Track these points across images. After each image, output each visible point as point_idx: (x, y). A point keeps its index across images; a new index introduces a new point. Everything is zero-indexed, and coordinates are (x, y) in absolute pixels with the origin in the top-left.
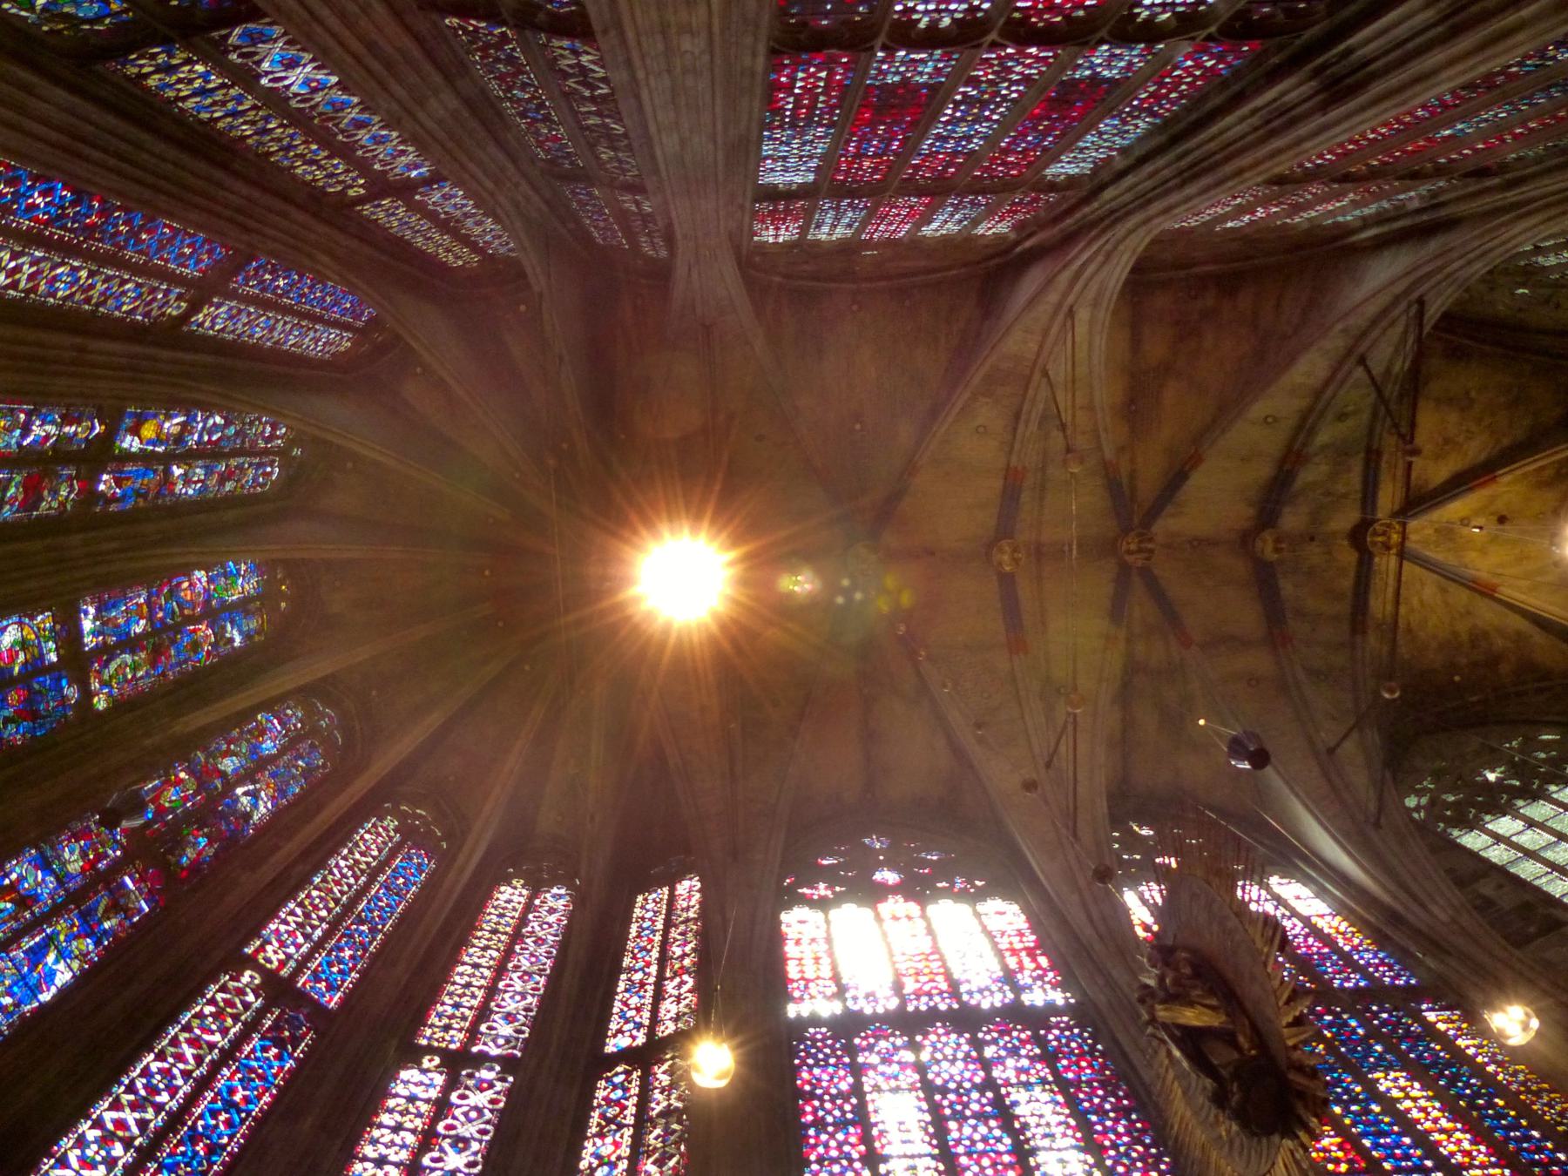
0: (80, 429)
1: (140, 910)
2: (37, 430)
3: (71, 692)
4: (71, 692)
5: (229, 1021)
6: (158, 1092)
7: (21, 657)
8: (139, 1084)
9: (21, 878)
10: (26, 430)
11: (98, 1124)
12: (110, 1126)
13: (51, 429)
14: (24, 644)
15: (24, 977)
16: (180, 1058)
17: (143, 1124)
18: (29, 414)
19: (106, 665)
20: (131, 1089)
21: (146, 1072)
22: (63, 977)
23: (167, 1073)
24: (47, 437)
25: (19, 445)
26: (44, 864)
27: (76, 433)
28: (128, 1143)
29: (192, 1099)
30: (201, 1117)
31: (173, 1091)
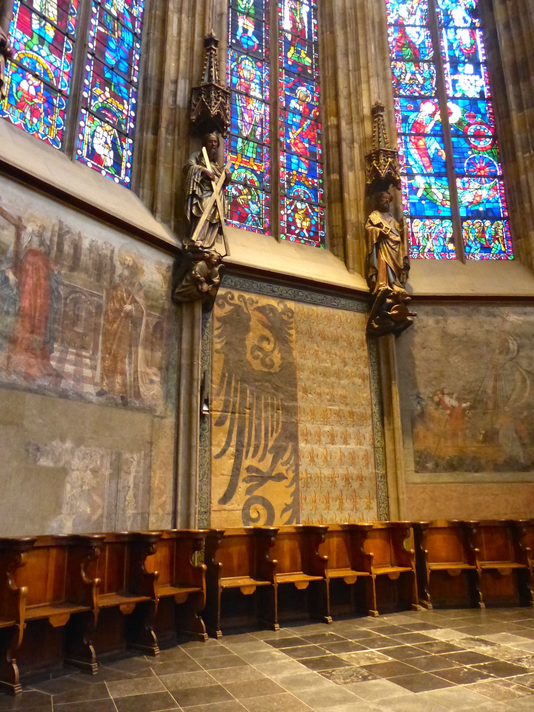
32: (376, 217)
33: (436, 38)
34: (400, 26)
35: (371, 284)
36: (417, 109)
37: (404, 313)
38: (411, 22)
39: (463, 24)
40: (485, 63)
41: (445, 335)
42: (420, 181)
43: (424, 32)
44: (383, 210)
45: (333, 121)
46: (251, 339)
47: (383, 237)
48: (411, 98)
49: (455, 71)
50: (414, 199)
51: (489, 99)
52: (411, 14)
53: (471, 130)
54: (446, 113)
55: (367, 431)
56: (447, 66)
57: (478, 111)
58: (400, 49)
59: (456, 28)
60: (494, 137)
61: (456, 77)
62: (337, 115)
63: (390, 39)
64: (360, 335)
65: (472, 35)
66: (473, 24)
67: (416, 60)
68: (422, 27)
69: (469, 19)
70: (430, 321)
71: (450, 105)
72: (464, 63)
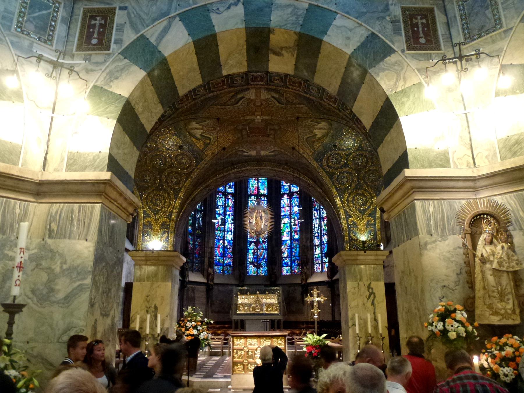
32: (209, 269)
35: (208, 281)
36: (219, 242)
37: (212, 287)
41: (219, 290)
42: (218, 258)
44: (211, 268)
45: (204, 247)
46: (190, 293)
47: (210, 273)
48: (218, 239)
49: (227, 234)
50: (216, 261)
53: (228, 247)
54: (224, 243)
55: (205, 307)
57: (230, 243)
62: (205, 246)
64: (205, 290)
67: (220, 231)
70: (216, 287)
71: (225, 241)
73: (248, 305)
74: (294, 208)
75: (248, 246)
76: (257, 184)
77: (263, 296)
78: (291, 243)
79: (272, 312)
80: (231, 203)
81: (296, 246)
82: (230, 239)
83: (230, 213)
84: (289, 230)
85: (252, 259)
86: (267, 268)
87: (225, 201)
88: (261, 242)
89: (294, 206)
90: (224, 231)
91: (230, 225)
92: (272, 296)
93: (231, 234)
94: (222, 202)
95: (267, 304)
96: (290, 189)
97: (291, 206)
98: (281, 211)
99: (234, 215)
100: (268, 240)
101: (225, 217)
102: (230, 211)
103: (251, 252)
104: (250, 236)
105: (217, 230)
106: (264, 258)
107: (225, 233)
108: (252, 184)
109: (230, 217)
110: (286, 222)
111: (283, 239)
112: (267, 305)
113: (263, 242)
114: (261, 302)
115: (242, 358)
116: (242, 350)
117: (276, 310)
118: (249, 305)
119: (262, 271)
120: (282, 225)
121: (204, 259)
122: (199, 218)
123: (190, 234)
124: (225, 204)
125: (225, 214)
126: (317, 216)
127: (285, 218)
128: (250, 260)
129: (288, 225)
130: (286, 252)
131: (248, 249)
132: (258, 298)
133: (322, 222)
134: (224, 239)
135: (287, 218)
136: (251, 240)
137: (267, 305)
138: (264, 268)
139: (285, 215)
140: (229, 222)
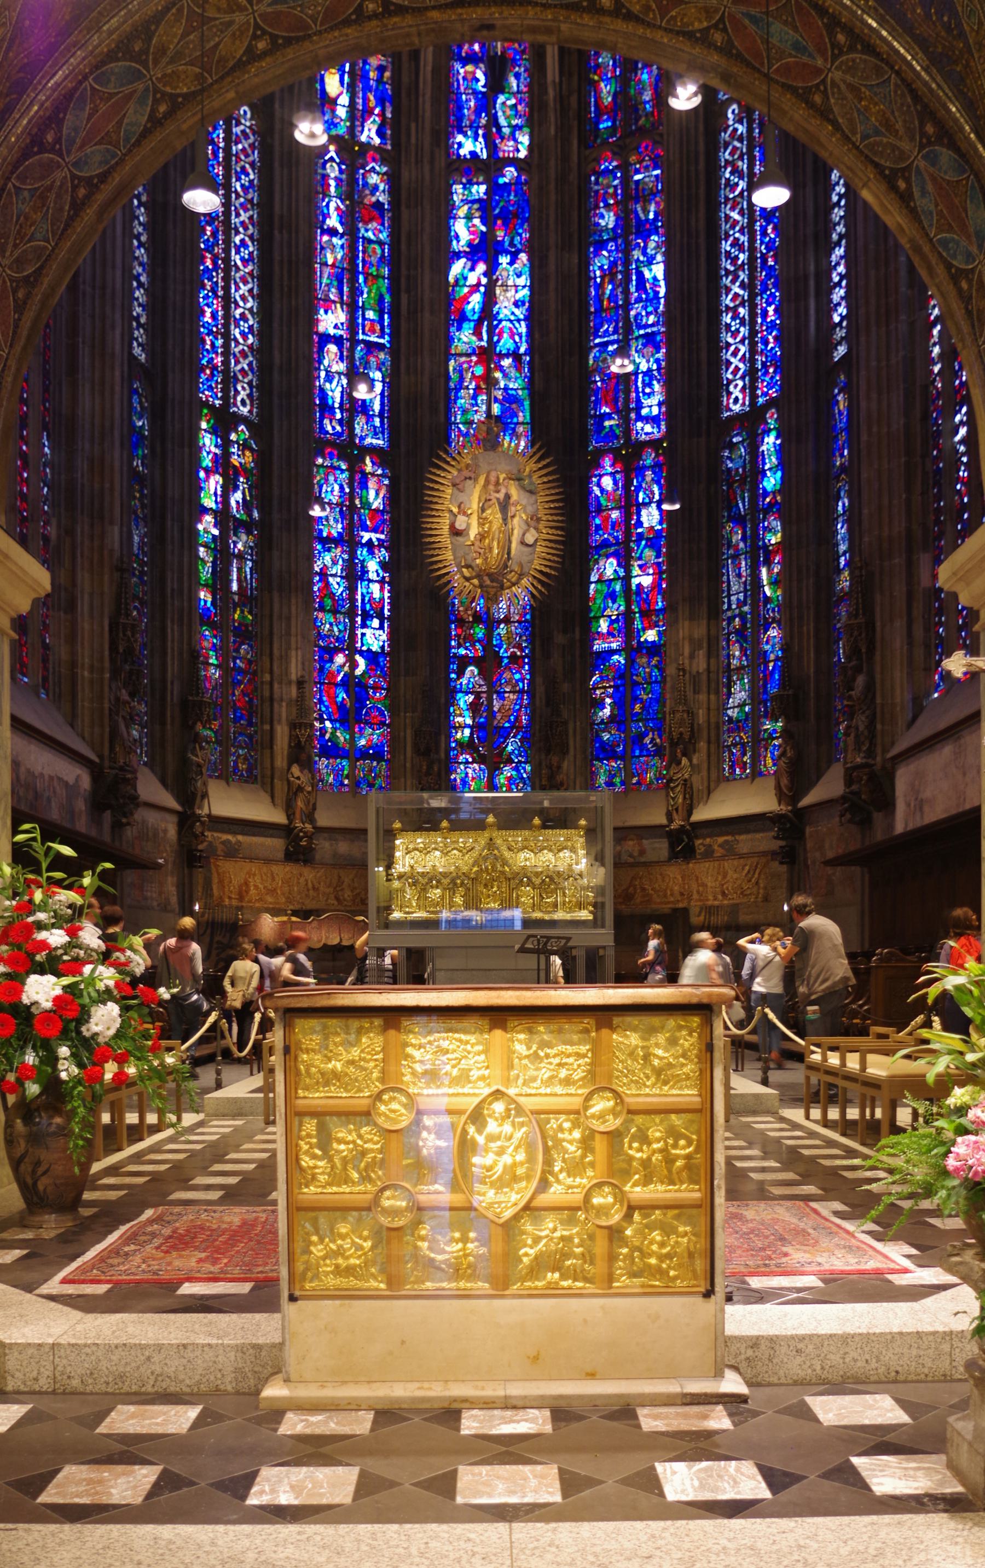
0: (332, 175)
1: (657, 176)
2: (333, 221)
3: (510, 173)
4: (510, 173)
5: (740, 163)
6: (737, 258)
7: (477, 221)
8: (729, 267)
9: (601, 268)
10: (332, 232)
11: (728, 309)
12: (732, 305)
13: (332, 206)
14: (469, 217)
15: (647, 300)
16: (736, 222)
17: (742, 286)
18: (323, 233)
19: (499, 128)
20: (728, 272)
21: (728, 254)
22: (658, 270)
23: (735, 243)
24: (338, 209)
25: (342, 236)
26: (601, 245)
27: (336, 179)
28: (742, 304)
29: (752, 240)
30: (762, 243)
31: (741, 250)
33: (352, 589)
34: (323, 574)
38: (334, 572)
39: (375, 578)
40: (389, 618)
43: (344, 584)
49: (364, 625)
51: (388, 654)
52: (335, 562)
56: (359, 619)
57: (378, 664)
58: (322, 598)
59: (370, 581)
60: (388, 690)
61: (364, 631)
63: (316, 589)
65: (382, 590)
66: (384, 578)
68: (341, 577)
69: (380, 571)
72: (372, 617)
73: (446, 881)
74: (644, 512)
75: (453, 676)
76: (484, 408)
77: (518, 837)
78: (631, 661)
79: (560, 915)
80: (375, 498)
81: (650, 674)
82: (375, 648)
83: (374, 536)
84: (622, 608)
85: (467, 732)
86: (528, 768)
87: (351, 485)
88: (506, 661)
89: (646, 505)
90: (352, 614)
91: (375, 588)
92: (560, 835)
93: (381, 627)
94: (337, 488)
95: (537, 874)
96: (628, 431)
97: (630, 506)
98: (588, 526)
99: (392, 545)
100: (532, 651)
101: (353, 555)
102: (375, 530)
103: (464, 700)
104: (458, 636)
105: (322, 608)
106: (516, 725)
107: (353, 622)
108: (465, 412)
109: (371, 552)
110: (609, 573)
111: (598, 646)
112: (537, 881)
113: (513, 657)
114: (505, 863)
115: (365, 1178)
116: (366, 1115)
117: (580, 906)
118: (451, 882)
119: (509, 779)
120: (593, 586)
121: (272, 730)
122: (241, 557)
123: (206, 618)
124: (352, 496)
125: (348, 541)
126: (742, 545)
127: (608, 557)
128: (459, 735)
129: (618, 587)
130: (608, 701)
131: (455, 691)
132: (491, 844)
133: (764, 571)
134: (351, 647)
135: (615, 555)
136: (462, 651)
137: (537, 881)
138: (516, 769)
139: (606, 544)
140: (373, 576)
